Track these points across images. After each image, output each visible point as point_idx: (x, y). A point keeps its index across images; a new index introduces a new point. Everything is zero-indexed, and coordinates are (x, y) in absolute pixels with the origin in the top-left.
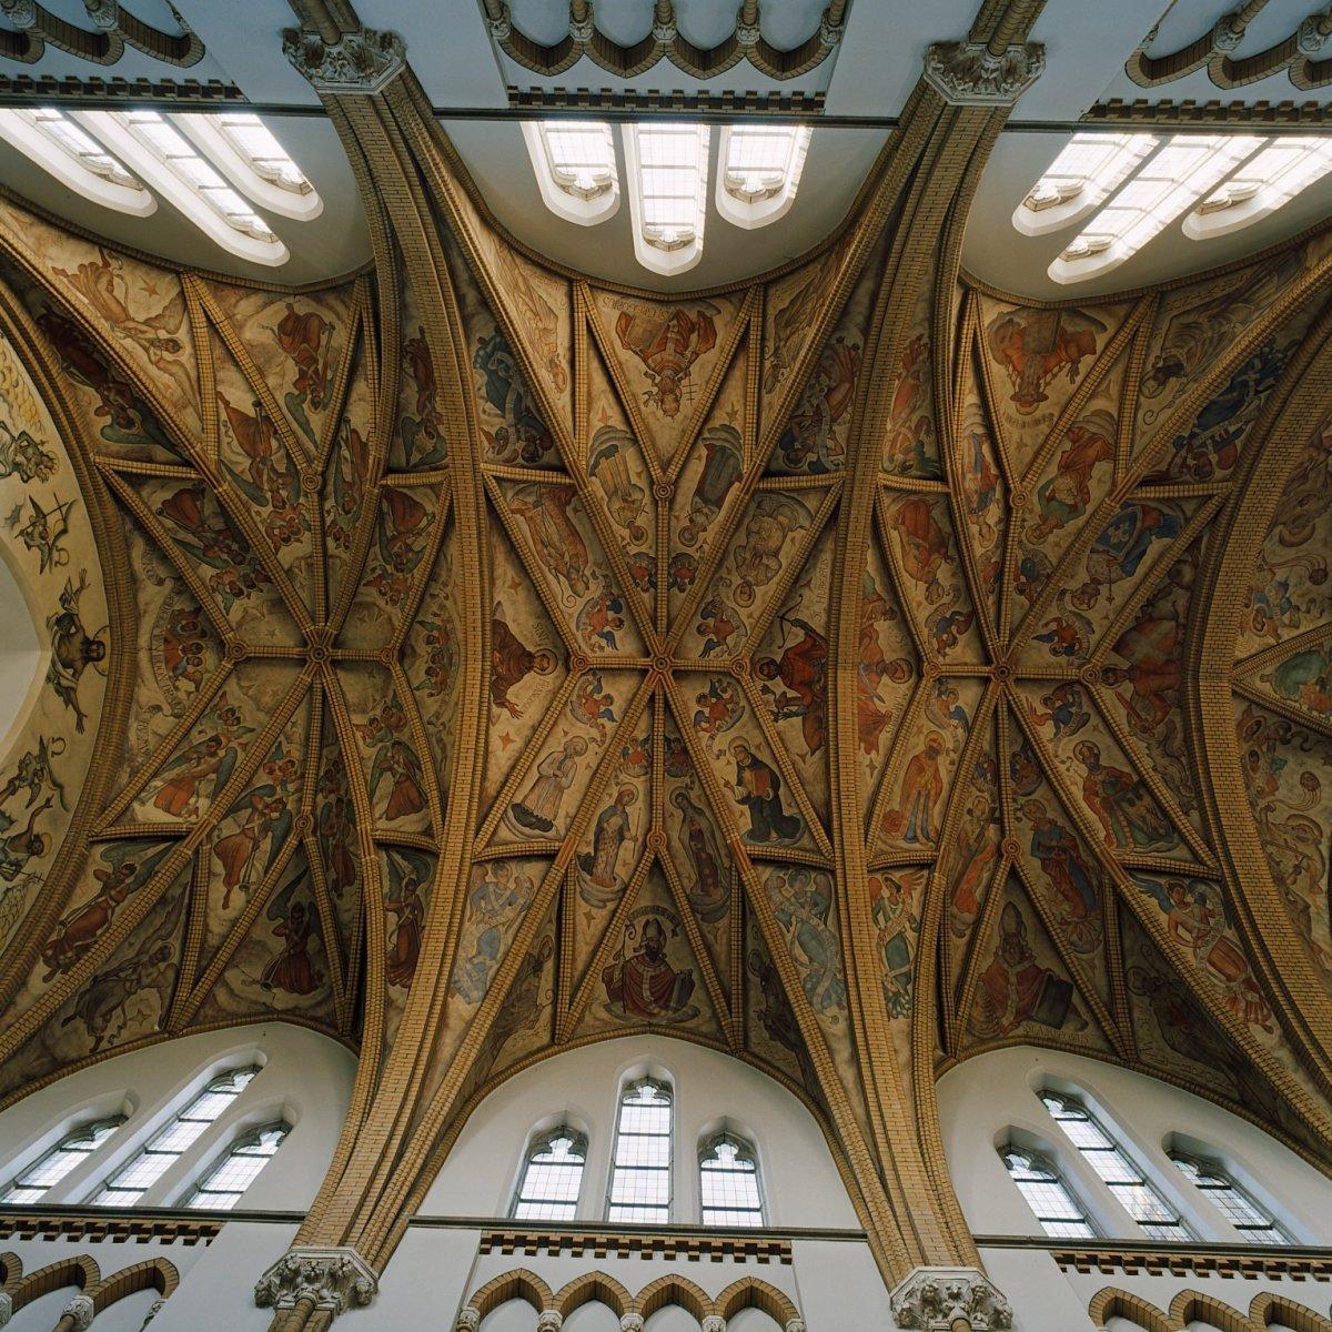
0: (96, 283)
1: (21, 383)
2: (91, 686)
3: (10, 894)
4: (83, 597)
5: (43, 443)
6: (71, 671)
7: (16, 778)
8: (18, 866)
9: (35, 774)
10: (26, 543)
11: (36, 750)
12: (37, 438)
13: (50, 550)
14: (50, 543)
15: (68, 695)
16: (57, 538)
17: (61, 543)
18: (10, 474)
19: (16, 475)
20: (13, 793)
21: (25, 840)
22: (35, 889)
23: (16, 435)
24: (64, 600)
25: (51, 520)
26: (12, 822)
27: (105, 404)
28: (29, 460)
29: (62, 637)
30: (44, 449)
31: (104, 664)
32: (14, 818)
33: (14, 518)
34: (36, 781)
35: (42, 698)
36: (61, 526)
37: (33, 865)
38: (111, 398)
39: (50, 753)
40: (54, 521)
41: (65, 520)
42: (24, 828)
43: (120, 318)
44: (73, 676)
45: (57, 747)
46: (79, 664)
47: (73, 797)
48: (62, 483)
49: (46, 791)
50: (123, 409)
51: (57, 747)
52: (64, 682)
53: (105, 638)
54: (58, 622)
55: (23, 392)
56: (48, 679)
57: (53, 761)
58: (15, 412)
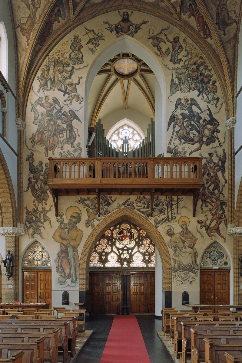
0: (25, 29)
1: (58, 49)
2: (136, 18)
3: (186, 49)
4: (111, 23)
5: (71, 41)
6: (131, 27)
7: (157, 48)
8: (180, 46)
9: (157, 41)
10: (98, 46)
11: (151, 40)
12: (70, 43)
13: (99, 37)
14: (97, 37)
15: (138, 28)
16: (95, 34)
17: (97, 33)
18: (81, 52)
19: (81, 50)
20: (161, 48)
21: (174, 44)
22: (189, 41)
23: (71, 50)
24: (112, 31)
25: (91, 37)
26: (168, 49)
27: (56, 20)
28: (77, 46)
29: (122, 31)
30: (73, 40)
31: (129, 12)
32: (167, 48)
33: (92, 50)
34: (159, 40)
35: (137, 39)
36: (92, 32)
37: (181, 41)
38: (54, 19)
39: (153, 35)
40: (91, 36)
41: (90, 31)
42: (171, 44)
43: (32, 18)
44: (132, 26)
45: (151, 32)
46: (129, 24)
47: (165, 24)
48: (79, 31)
49: (162, 36)
50: (56, 14)
51: (151, 32)
52: (134, 30)
53: (122, 11)
54: (117, 33)
55: (60, 48)
56: (133, 36)
57: (155, 33)
58: (66, 51)
